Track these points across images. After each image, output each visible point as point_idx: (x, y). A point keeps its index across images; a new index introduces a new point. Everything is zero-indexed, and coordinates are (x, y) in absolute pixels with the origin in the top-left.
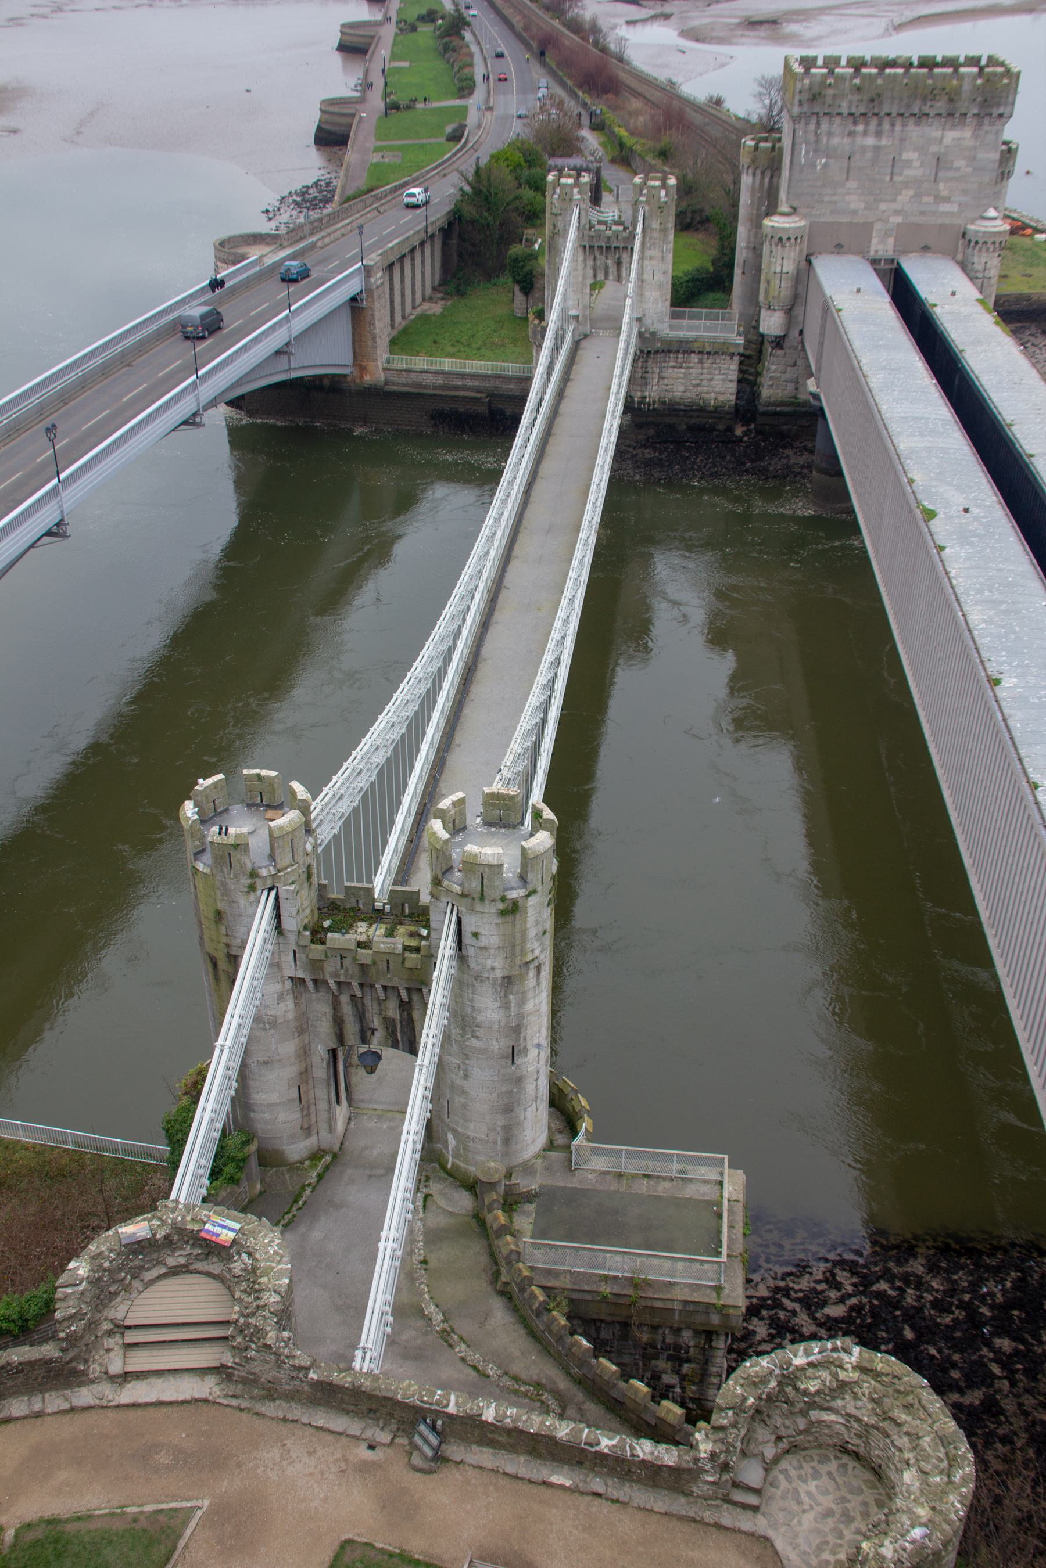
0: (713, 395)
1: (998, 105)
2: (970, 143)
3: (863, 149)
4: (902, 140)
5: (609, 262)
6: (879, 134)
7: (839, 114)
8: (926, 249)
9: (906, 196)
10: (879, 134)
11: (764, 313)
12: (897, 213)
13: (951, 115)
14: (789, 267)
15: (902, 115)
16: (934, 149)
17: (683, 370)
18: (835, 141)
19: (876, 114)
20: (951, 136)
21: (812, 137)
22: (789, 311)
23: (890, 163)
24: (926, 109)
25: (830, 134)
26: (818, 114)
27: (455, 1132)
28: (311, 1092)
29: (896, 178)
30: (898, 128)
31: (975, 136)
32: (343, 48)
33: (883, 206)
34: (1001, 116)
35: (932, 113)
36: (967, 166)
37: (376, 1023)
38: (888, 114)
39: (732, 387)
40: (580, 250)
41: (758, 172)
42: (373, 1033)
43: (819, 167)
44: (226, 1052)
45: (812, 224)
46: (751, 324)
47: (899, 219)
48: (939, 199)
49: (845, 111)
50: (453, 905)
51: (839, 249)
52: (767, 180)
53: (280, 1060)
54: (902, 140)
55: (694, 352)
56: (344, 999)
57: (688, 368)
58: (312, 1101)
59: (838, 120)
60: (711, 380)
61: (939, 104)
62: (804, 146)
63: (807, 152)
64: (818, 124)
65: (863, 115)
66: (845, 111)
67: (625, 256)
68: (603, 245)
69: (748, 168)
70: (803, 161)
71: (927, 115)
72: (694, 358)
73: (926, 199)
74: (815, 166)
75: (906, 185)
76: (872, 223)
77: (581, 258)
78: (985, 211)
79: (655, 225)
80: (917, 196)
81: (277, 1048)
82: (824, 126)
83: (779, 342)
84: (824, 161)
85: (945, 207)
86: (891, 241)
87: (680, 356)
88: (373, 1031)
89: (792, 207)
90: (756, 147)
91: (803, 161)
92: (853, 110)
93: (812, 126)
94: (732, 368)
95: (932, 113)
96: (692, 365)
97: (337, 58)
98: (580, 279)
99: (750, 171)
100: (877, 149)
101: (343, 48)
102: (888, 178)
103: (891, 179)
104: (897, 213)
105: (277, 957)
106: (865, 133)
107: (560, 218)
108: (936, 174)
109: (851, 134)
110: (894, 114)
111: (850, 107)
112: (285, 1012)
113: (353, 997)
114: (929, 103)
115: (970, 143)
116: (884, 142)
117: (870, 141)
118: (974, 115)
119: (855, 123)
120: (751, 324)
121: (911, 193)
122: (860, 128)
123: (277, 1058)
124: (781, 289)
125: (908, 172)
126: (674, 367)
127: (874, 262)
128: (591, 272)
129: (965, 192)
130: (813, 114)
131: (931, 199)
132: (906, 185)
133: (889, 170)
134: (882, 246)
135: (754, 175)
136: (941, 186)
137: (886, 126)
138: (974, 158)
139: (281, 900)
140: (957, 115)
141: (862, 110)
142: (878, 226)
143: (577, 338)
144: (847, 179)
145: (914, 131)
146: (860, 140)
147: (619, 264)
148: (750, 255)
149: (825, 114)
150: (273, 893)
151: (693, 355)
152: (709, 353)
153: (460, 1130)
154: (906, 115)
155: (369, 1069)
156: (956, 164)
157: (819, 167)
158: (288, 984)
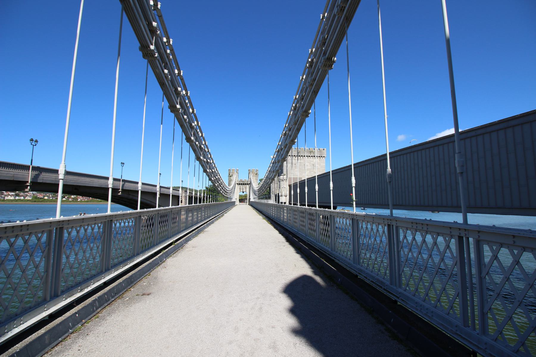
1: (323, 155)
2: (319, 162)
5: (244, 187)
16: (312, 163)
24: (310, 155)
31: (320, 161)
35: (311, 156)
36: (319, 166)
38: (302, 156)
61: (311, 154)
68: (242, 183)
71: (309, 156)
73: (312, 173)
75: (307, 170)
95: (311, 156)
102: (304, 168)
107: (232, 177)
111: (294, 154)
115: (319, 162)
116: (302, 161)
121: (309, 171)
128: (239, 190)
131: (313, 173)
132: (307, 170)
133: (304, 167)
138: (320, 165)
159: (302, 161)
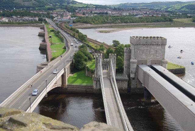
3: (145, 49)
4: (151, 48)
6: (147, 47)
8: (155, 64)
9: (152, 56)
10: (147, 47)
11: (131, 74)
12: (151, 58)
14: (135, 67)
16: (155, 49)
18: (141, 48)
20: (158, 47)
21: (137, 48)
22: (135, 74)
23: (149, 52)
25: (140, 47)
29: (150, 53)
30: (150, 46)
31: (162, 48)
32: (39, 35)
33: (149, 57)
34: (165, 45)
39: (127, 86)
45: (138, 60)
46: (129, 76)
47: (151, 59)
48: (157, 56)
51: (142, 64)
54: (151, 48)
59: (141, 46)
73: (155, 56)
76: (147, 60)
80: (154, 56)
82: (139, 46)
83: (134, 79)
85: (158, 57)
86: (150, 63)
90: (127, 49)
94: (127, 83)
97: (38, 37)
100: (147, 49)
101: (39, 35)
104: (151, 58)
106: (145, 47)
117: (146, 48)
120: (129, 76)
122: (144, 46)
124: (134, 71)
125: (152, 52)
127: (148, 66)
129: (161, 55)
132: (152, 54)
134: (149, 64)
137: (148, 46)
142: (148, 60)
145: (152, 47)
146: (144, 48)
147: (107, 67)
148: (127, 65)
156: (159, 51)
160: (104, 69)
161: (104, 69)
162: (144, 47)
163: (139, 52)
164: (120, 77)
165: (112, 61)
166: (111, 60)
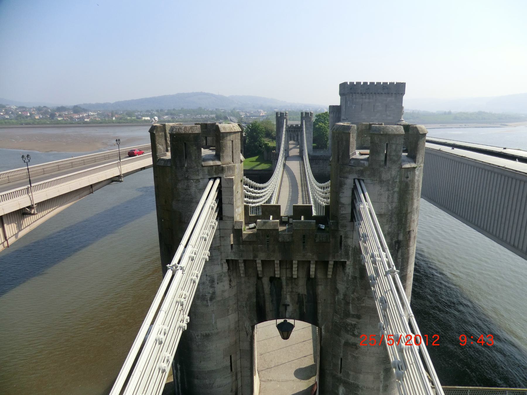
0: (327, 172)
6: (369, 98)
7: (358, 93)
10: (369, 98)
13: (388, 93)
15: (375, 93)
17: (318, 165)
19: (368, 93)
20: (389, 99)
26: (352, 93)
27: (346, 384)
28: (238, 362)
29: (375, 110)
30: (374, 97)
37: (288, 300)
38: (371, 93)
40: (286, 131)
41: (335, 113)
42: (286, 309)
43: (353, 107)
44: (179, 273)
49: (359, 92)
50: (359, 180)
52: (337, 115)
53: (217, 333)
55: (321, 160)
56: (266, 281)
57: (319, 164)
58: (239, 369)
60: (326, 168)
62: (349, 102)
63: (350, 103)
64: (352, 96)
65: (364, 93)
66: (359, 92)
67: (299, 133)
68: (293, 130)
69: (332, 112)
70: (349, 105)
71: (382, 93)
72: (321, 161)
73: (384, 116)
74: (352, 107)
77: (287, 134)
78: (400, 119)
79: (308, 124)
81: (216, 323)
82: (354, 96)
84: (354, 106)
87: (317, 161)
88: (286, 306)
89: (346, 118)
91: (349, 105)
92: (362, 92)
93: (351, 97)
96: (320, 163)
98: (286, 140)
99: (332, 113)
102: (373, 110)
103: (374, 111)
105: (218, 241)
106: (365, 98)
108: (386, 109)
109: (362, 98)
110: (373, 93)
112: (223, 291)
113: (272, 279)
114: (382, 90)
116: (371, 101)
117: (367, 100)
118: (395, 93)
119: (363, 95)
122: (364, 97)
123: (216, 331)
126: (315, 164)
130: (351, 93)
135: (333, 113)
136: (388, 112)
139: (223, 189)
140: (390, 93)
141: (365, 92)
143: (286, 156)
144: (362, 111)
147: (298, 136)
149: (354, 93)
150: (218, 181)
151: (320, 161)
152: (325, 160)
153: (351, 381)
154: (377, 93)
155: (285, 336)
157: (353, 107)
158: (225, 266)
159: (371, 101)
160: (292, 139)
161: (292, 139)
162: (362, 98)
163: (355, 107)
164: (320, 153)
165: (306, 124)
166: (304, 123)
